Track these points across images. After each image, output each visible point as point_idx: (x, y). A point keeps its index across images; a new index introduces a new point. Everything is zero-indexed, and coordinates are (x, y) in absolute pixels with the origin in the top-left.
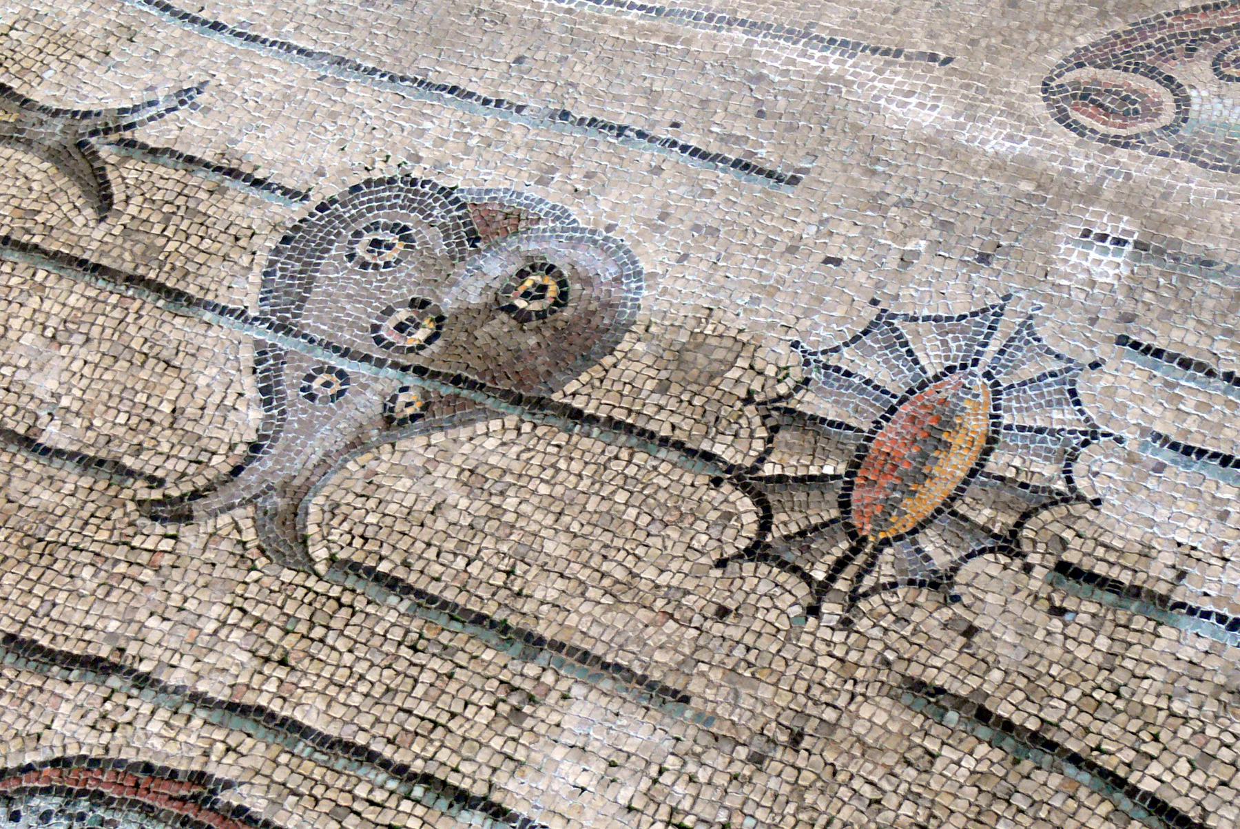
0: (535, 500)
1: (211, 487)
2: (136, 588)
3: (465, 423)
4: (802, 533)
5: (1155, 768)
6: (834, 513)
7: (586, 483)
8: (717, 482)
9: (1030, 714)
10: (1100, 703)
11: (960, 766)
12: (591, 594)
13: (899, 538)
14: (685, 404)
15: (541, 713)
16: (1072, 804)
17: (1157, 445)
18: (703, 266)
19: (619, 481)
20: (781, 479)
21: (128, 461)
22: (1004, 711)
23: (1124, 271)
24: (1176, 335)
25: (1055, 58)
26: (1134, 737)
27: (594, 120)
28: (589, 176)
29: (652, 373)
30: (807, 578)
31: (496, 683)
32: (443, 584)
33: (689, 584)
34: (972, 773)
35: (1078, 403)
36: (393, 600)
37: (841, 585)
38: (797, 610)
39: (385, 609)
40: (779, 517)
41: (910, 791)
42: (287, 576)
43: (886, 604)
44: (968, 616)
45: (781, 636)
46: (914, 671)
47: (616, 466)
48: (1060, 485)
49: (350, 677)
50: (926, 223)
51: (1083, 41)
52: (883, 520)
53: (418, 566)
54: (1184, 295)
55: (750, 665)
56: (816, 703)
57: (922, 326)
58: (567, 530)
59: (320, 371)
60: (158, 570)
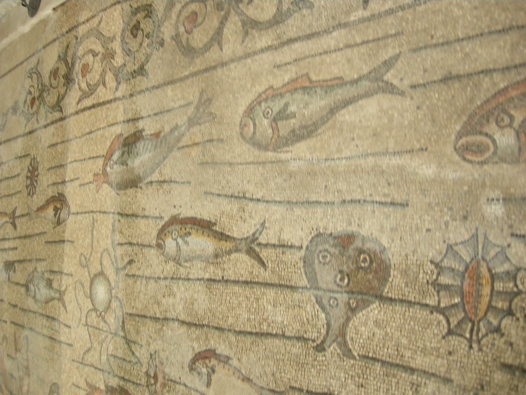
3: (368, 306)
8: (432, 313)
20: (446, 308)
23: (503, 210)
25: (453, 137)
33: (439, 345)
37: (474, 338)
46: (502, 360)
48: (515, 289)
51: (458, 128)
52: (476, 315)
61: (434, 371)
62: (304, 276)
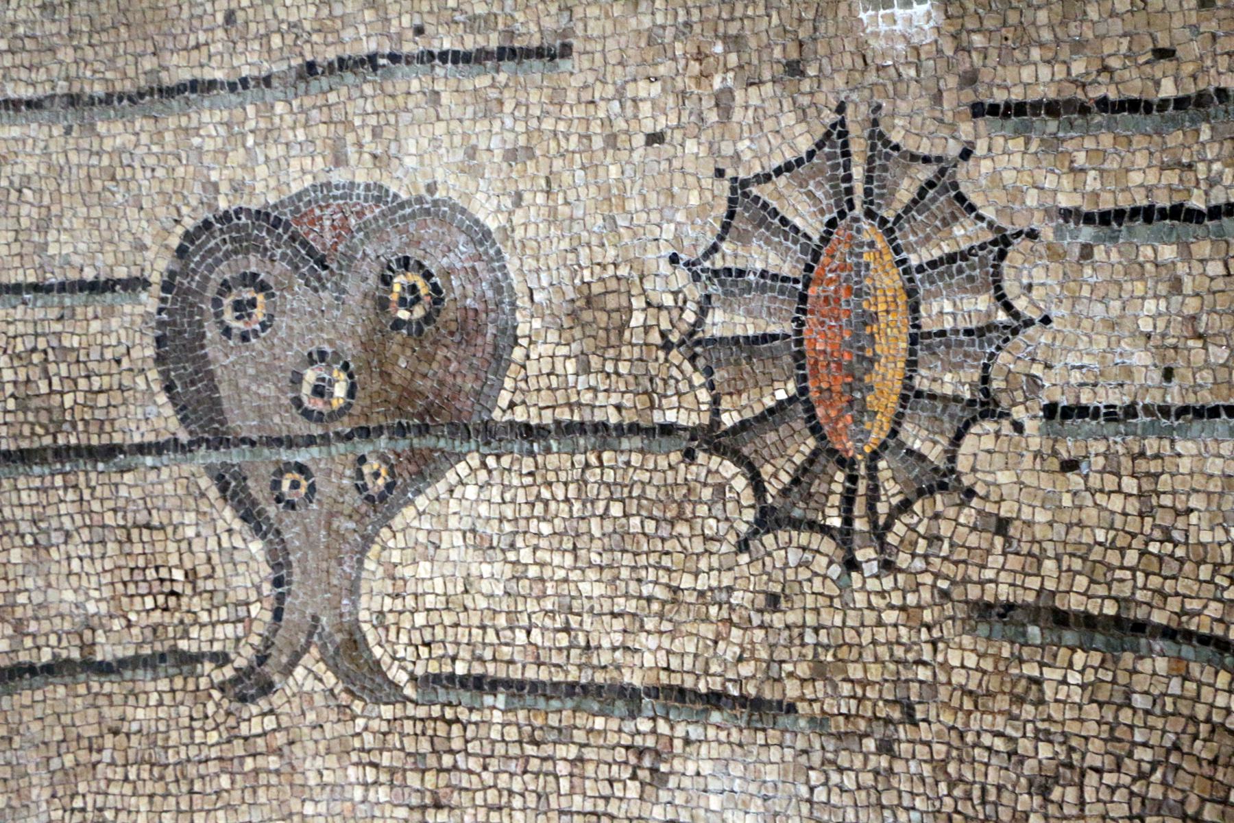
0: (543, 543)
1: (268, 643)
2: (274, 780)
3: (438, 475)
4: (796, 481)
6: (811, 443)
7: (577, 506)
8: (689, 455)
9: (1103, 598)
10: (1160, 558)
11: (1068, 684)
12: (650, 624)
13: (884, 446)
14: (614, 377)
15: (677, 765)
16: (1191, 686)
17: (1072, 225)
18: (540, 199)
19: (605, 493)
20: (743, 426)
21: (183, 645)
22: (1075, 603)
24: (1027, 74)
26: (1212, 587)
27: (341, 60)
28: (376, 133)
29: (564, 350)
30: (826, 530)
31: (623, 751)
32: (519, 666)
33: (727, 580)
34: (1083, 686)
35: (972, 208)
36: (488, 700)
37: (860, 525)
38: (835, 571)
39: (487, 712)
40: (766, 470)
41: (1037, 730)
42: (387, 711)
43: (912, 528)
44: (990, 508)
45: (837, 603)
46: (974, 592)
47: (593, 476)
49: (500, 796)
50: (719, 48)
53: (488, 654)
54: (1013, 18)
55: (827, 647)
56: (904, 662)
57: (782, 181)
58: (591, 565)
59: (280, 473)
60: (279, 752)
61: (715, 683)
62: (162, 398)
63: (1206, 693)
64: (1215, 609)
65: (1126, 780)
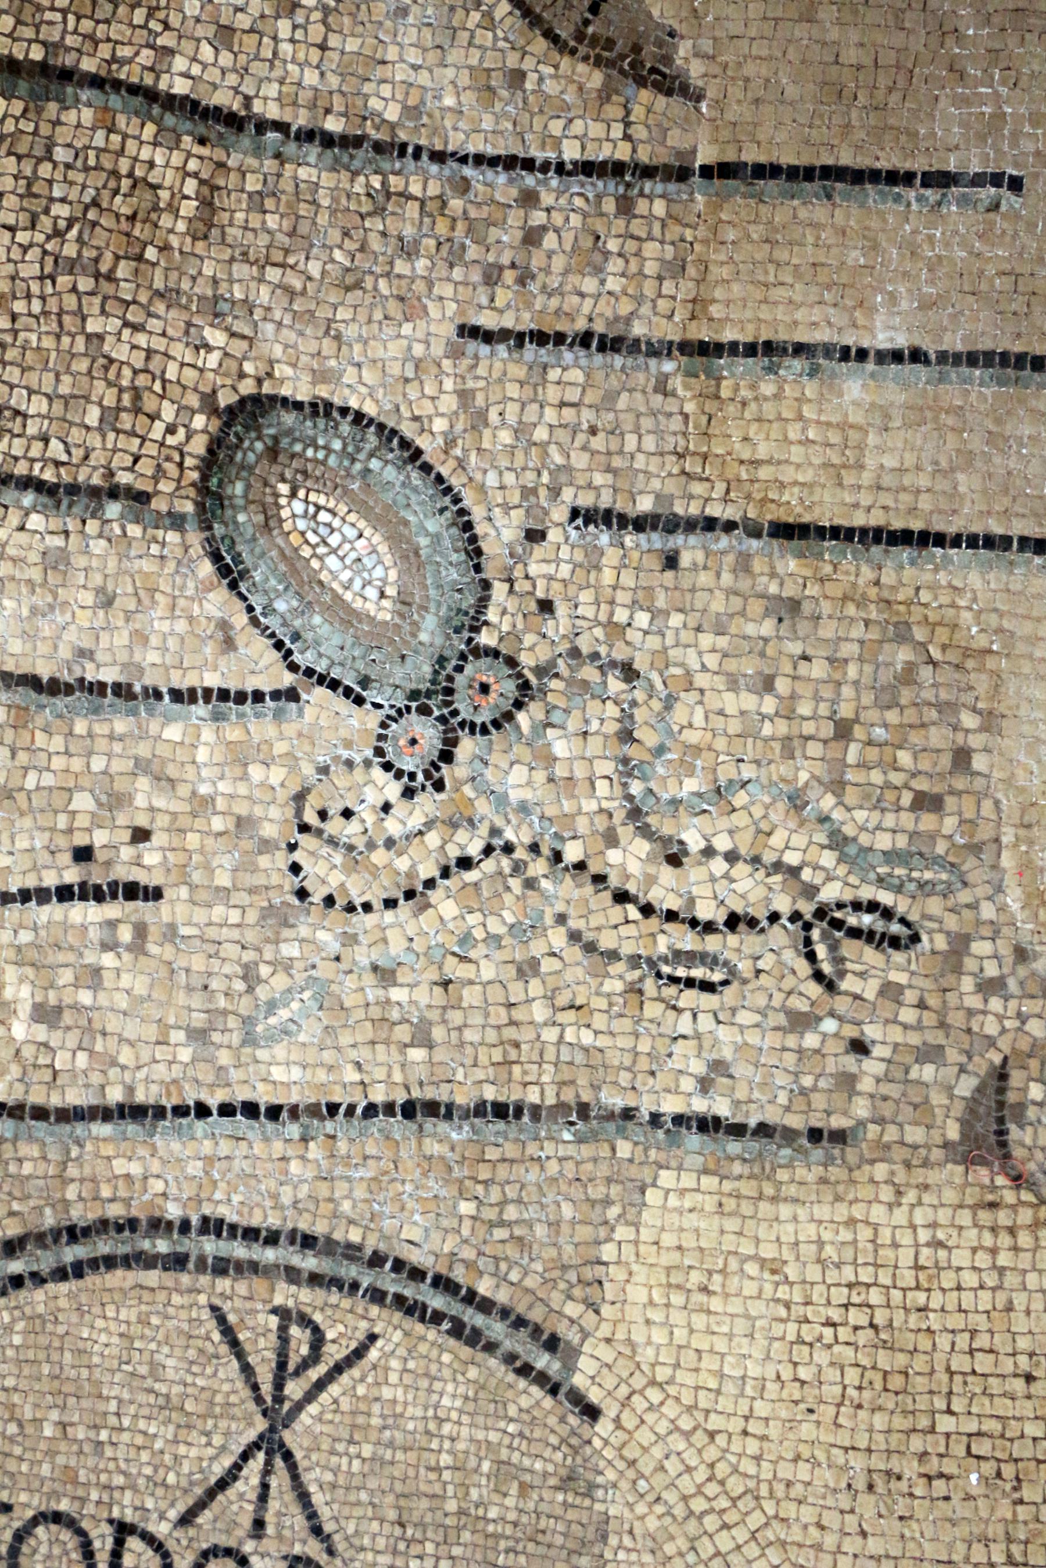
5: (180, 63)
9: (30, 42)
16: (116, 138)
26: (145, 32)
63: (131, 146)
64: (146, 57)
65: (40, 238)
